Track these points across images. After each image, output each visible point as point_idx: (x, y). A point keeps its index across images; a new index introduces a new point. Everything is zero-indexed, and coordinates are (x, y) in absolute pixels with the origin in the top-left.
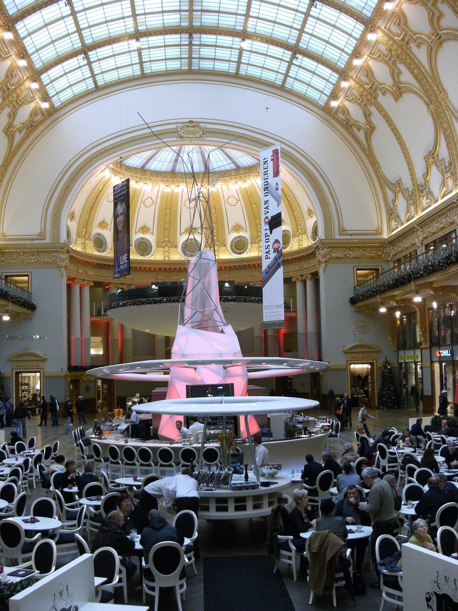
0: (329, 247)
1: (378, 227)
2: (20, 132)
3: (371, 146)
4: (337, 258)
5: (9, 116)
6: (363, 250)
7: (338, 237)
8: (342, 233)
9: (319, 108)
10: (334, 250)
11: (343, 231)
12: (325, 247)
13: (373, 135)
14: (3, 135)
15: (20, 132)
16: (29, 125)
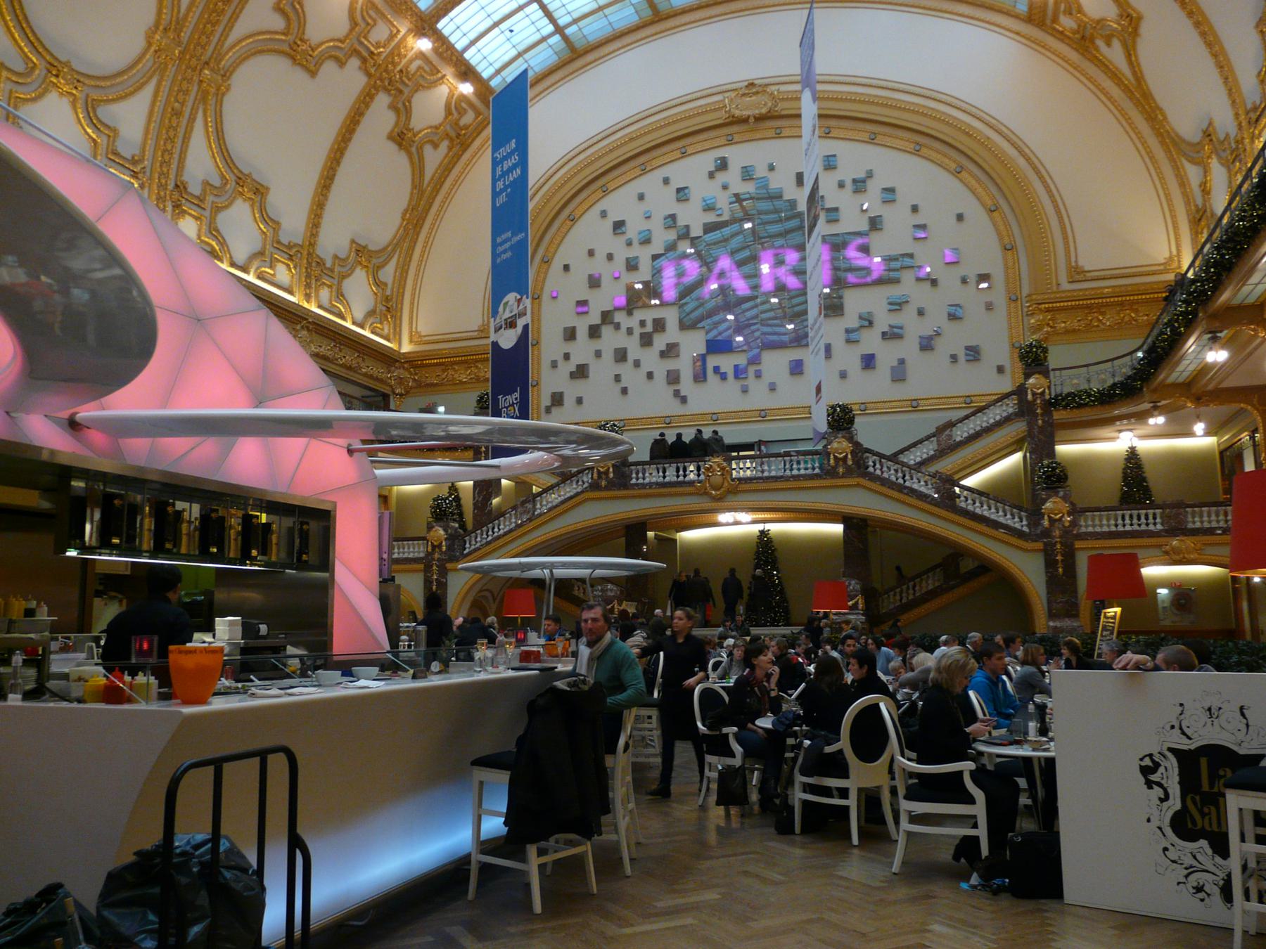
0: (1048, 310)
1: (1171, 258)
2: (436, 146)
3: (1139, 65)
4: (1067, 332)
5: (393, 107)
6: (1132, 310)
7: (1066, 286)
8: (1077, 277)
9: (1017, 17)
10: (1060, 317)
11: (1077, 273)
12: (1040, 310)
13: (1139, 40)
14: (392, 147)
15: (436, 146)
16: (453, 134)
